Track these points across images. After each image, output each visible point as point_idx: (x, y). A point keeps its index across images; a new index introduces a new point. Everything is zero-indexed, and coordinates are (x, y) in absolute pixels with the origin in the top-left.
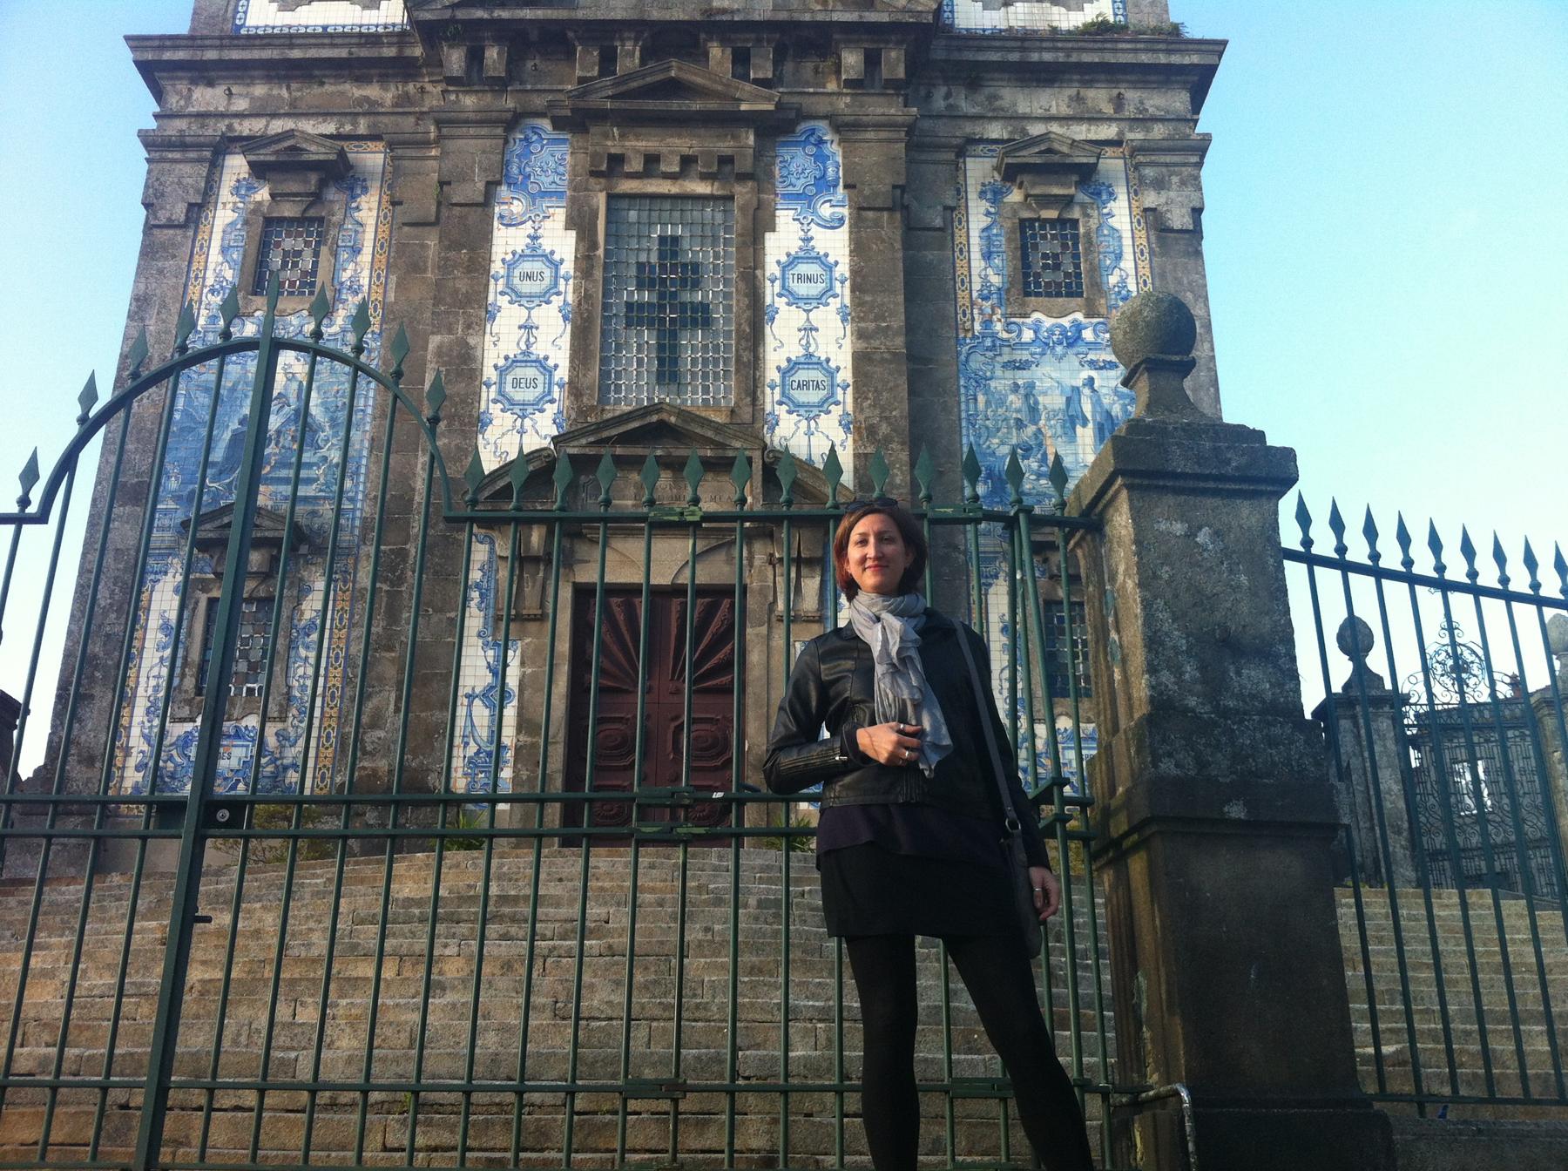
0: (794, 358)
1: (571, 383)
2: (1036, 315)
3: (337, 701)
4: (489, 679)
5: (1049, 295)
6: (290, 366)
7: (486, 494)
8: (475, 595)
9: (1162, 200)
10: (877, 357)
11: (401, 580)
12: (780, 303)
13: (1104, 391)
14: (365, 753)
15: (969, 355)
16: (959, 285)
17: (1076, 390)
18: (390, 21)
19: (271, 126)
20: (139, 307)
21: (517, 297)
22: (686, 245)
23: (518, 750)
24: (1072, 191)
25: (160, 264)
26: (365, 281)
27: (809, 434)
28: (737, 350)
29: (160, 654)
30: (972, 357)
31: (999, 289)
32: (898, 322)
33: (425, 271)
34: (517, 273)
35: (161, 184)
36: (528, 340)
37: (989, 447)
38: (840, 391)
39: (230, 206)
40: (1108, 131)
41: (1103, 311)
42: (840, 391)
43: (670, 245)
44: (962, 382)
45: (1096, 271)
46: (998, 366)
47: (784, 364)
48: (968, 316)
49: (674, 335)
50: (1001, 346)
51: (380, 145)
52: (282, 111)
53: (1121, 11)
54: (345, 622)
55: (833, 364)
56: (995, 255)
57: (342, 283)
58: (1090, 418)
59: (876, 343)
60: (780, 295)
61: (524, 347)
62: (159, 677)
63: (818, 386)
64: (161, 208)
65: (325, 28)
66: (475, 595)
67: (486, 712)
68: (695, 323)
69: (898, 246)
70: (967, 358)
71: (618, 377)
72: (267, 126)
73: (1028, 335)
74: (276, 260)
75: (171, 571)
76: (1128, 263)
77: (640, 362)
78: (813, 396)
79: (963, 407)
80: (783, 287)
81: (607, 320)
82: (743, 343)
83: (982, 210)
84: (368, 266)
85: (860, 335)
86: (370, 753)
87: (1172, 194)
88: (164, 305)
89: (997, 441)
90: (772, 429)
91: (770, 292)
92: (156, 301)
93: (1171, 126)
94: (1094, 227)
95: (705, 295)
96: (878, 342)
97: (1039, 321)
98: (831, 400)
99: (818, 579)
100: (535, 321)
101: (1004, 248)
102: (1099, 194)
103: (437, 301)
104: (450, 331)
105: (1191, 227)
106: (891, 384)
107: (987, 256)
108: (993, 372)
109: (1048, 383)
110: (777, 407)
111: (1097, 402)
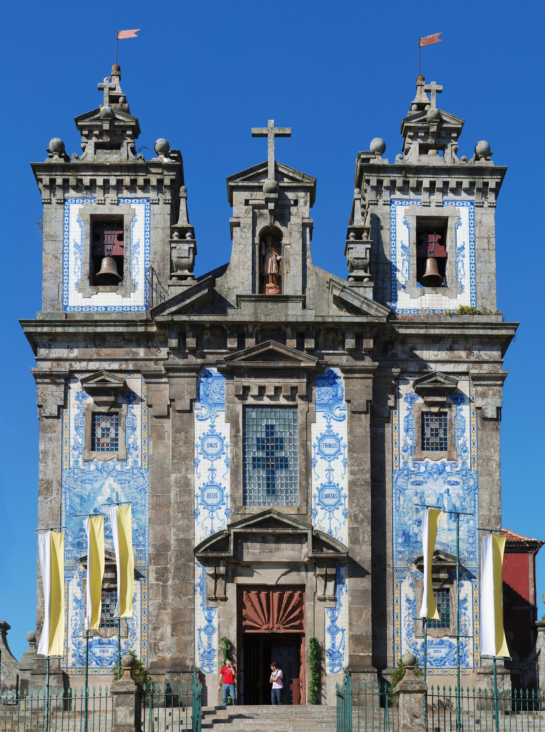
0: (324, 484)
1: (231, 496)
2: (426, 459)
3: (146, 629)
4: (206, 623)
5: (433, 449)
6: (112, 485)
7: (202, 549)
8: (198, 589)
9: (484, 403)
10: (359, 483)
11: (166, 581)
12: (318, 457)
13: (453, 495)
14: (159, 650)
15: (397, 478)
16: (394, 444)
17: (441, 495)
18: (136, 305)
19: (89, 365)
20: (43, 457)
21: (207, 456)
22: (277, 429)
23: (219, 651)
24: (444, 399)
25: (49, 435)
26: (139, 444)
27: (330, 518)
28: (300, 481)
29: (75, 611)
30: (399, 479)
31: (411, 447)
32: (367, 466)
33: (164, 439)
34: (206, 443)
35: (44, 395)
36: (212, 476)
37: (404, 521)
38: (343, 499)
39: (76, 406)
40: (462, 368)
41: (455, 457)
42: (343, 499)
43: (270, 428)
44: (394, 491)
45: (453, 437)
46: (409, 484)
47: (320, 487)
48: (398, 459)
49: (273, 472)
50: (411, 474)
51: (139, 375)
52: (94, 358)
53: (474, 298)
54: (146, 598)
55: (340, 486)
56: (410, 430)
57: (129, 445)
58: (446, 506)
59: (358, 477)
60: (318, 454)
61: (211, 479)
62: (76, 620)
63: (334, 497)
64: (46, 408)
65: (106, 308)
66: (198, 589)
67: (206, 636)
68: (282, 466)
69: (368, 430)
70: (396, 480)
71: (250, 493)
72: (88, 364)
73: (423, 469)
74: (99, 432)
75: (75, 577)
76: (467, 434)
77: (259, 485)
78: (332, 501)
79: (394, 503)
80: (319, 450)
81: (244, 466)
82: (303, 477)
83: (406, 408)
84: (139, 437)
85: (352, 473)
86: (161, 651)
87: (489, 400)
88: (54, 455)
89: (407, 518)
90: (315, 516)
91: (314, 452)
92: (50, 453)
93: (491, 365)
94: (454, 416)
95: (286, 454)
96: (359, 476)
97: (427, 462)
98: (339, 503)
99: (334, 582)
100: (215, 467)
101: (414, 426)
102: (457, 399)
103: (173, 458)
104: (180, 473)
105: (496, 417)
106: (364, 496)
107: (407, 430)
108: (407, 486)
109: (430, 491)
110: (317, 506)
111: (450, 501)
